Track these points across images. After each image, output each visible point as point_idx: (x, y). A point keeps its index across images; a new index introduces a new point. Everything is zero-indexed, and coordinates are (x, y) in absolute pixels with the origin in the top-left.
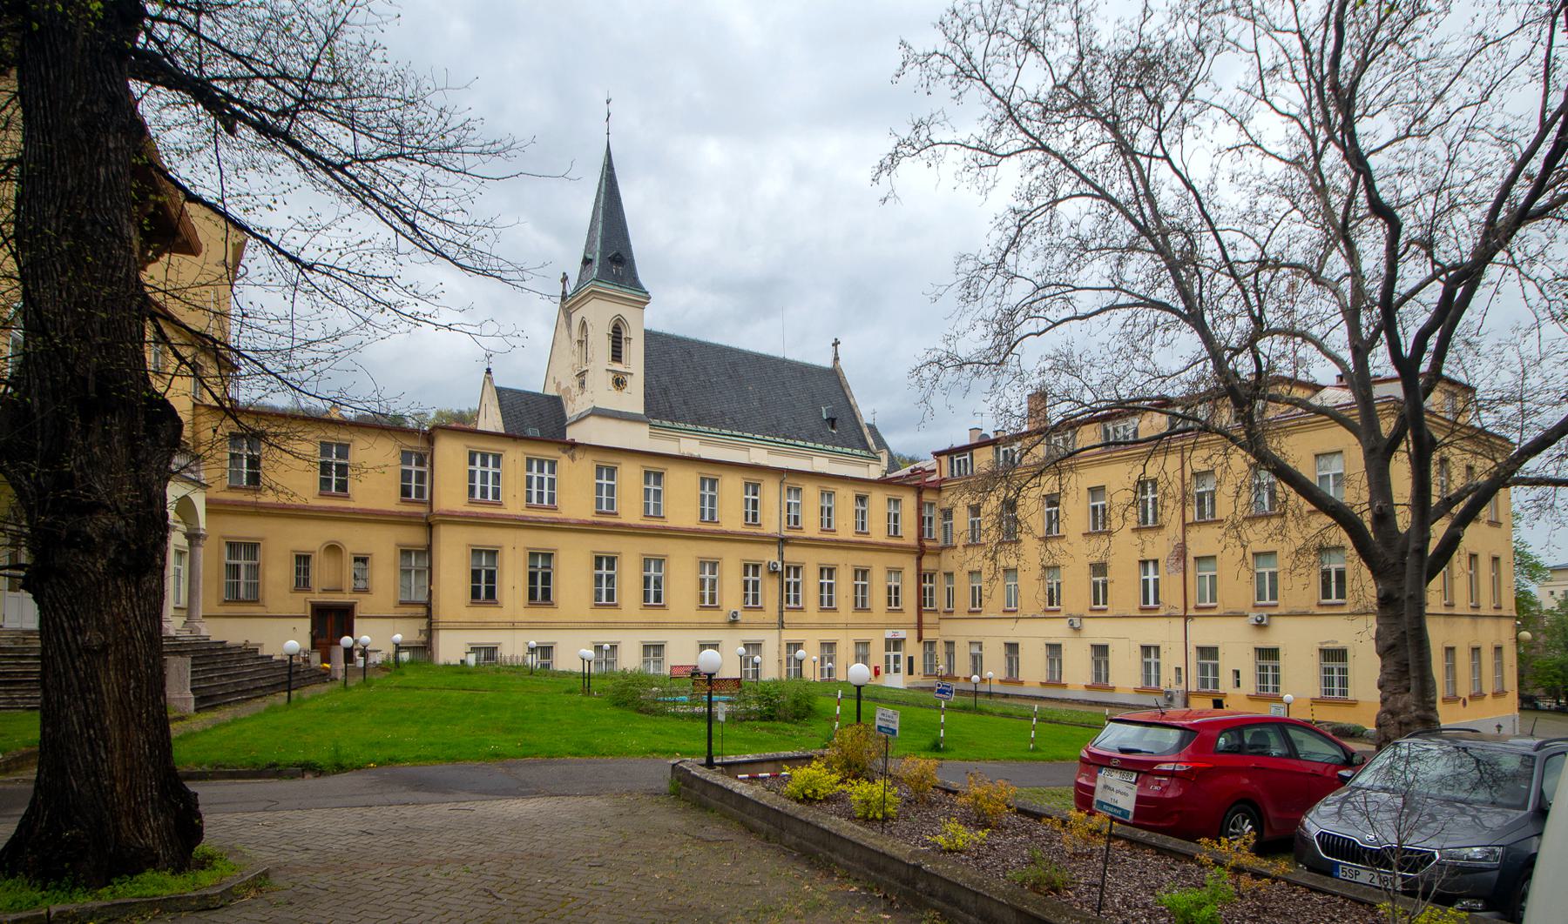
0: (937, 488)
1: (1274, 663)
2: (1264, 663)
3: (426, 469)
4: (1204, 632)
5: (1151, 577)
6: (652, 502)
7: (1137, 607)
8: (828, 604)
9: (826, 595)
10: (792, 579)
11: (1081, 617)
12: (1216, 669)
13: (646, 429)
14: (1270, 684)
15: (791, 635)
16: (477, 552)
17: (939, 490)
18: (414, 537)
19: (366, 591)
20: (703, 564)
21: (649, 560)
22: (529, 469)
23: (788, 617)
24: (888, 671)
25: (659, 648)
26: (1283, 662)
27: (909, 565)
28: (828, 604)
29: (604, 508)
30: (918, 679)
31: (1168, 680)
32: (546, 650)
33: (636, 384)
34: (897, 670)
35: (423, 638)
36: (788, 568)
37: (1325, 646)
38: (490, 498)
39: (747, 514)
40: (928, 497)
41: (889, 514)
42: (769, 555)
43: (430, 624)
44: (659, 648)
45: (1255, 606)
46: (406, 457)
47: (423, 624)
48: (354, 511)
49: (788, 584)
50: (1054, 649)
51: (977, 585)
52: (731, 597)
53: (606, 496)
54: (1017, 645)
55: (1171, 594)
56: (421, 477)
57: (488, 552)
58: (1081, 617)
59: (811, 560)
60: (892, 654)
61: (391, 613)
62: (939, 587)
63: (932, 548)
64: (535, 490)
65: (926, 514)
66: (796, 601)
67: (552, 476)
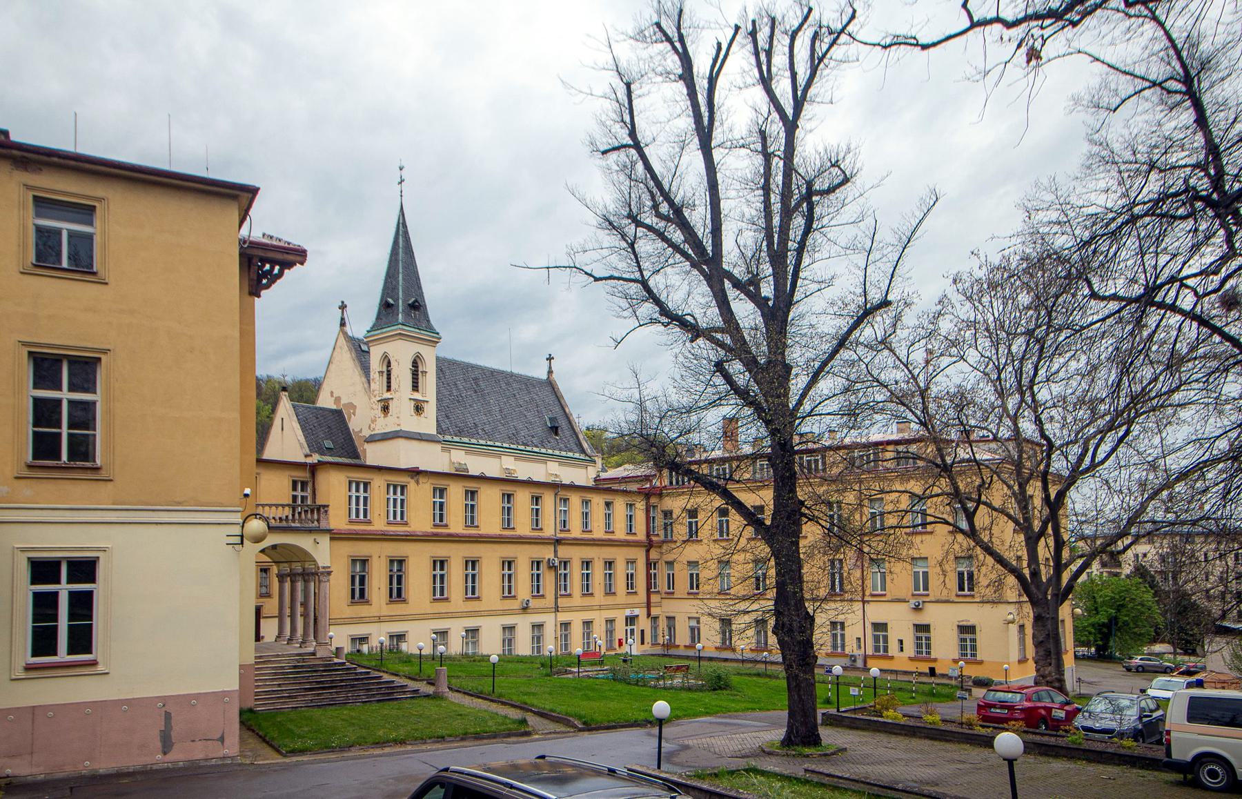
1: (927, 635)
2: (920, 634)
4: (877, 612)
10: (562, 571)
12: (886, 639)
14: (924, 650)
15: (563, 617)
17: (660, 495)
23: (562, 602)
26: (933, 634)
30: (647, 648)
31: (851, 647)
33: (431, 409)
37: (961, 624)
42: (547, 553)
45: (913, 595)
51: (695, 572)
59: (575, 555)
60: (629, 628)
62: (662, 573)
65: (652, 514)
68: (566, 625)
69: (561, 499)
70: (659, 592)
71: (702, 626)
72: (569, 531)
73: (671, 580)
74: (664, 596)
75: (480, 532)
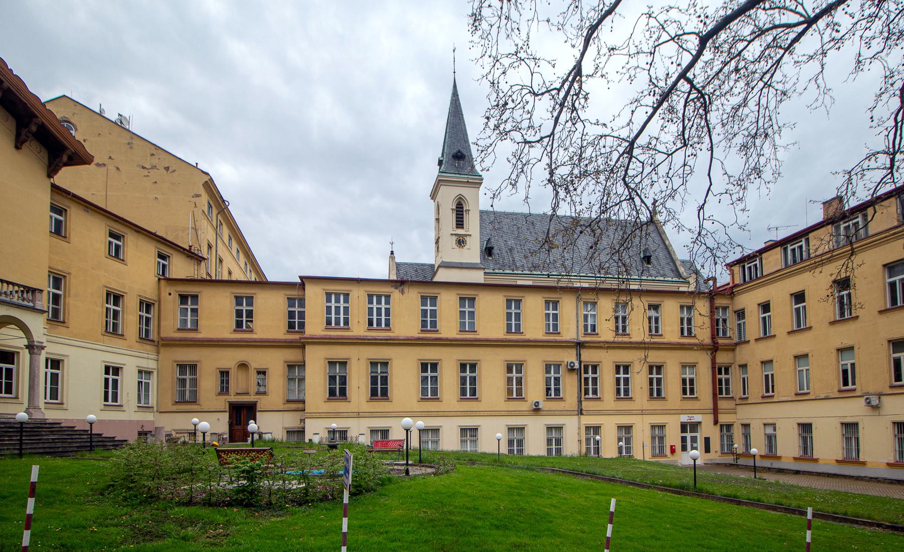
10: (590, 375)
18: (292, 355)
22: (371, 302)
24: (684, 448)
25: (474, 430)
27: (703, 362)
30: (715, 455)
36: (586, 367)
40: (720, 302)
42: (569, 357)
44: (474, 430)
49: (586, 379)
51: (770, 373)
52: (534, 389)
53: (429, 321)
57: (340, 363)
59: (607, 360)
60: (689, 435)
69: (586, 303)
70: (733, 398)
72: (597, 334)
75: (478, 337)
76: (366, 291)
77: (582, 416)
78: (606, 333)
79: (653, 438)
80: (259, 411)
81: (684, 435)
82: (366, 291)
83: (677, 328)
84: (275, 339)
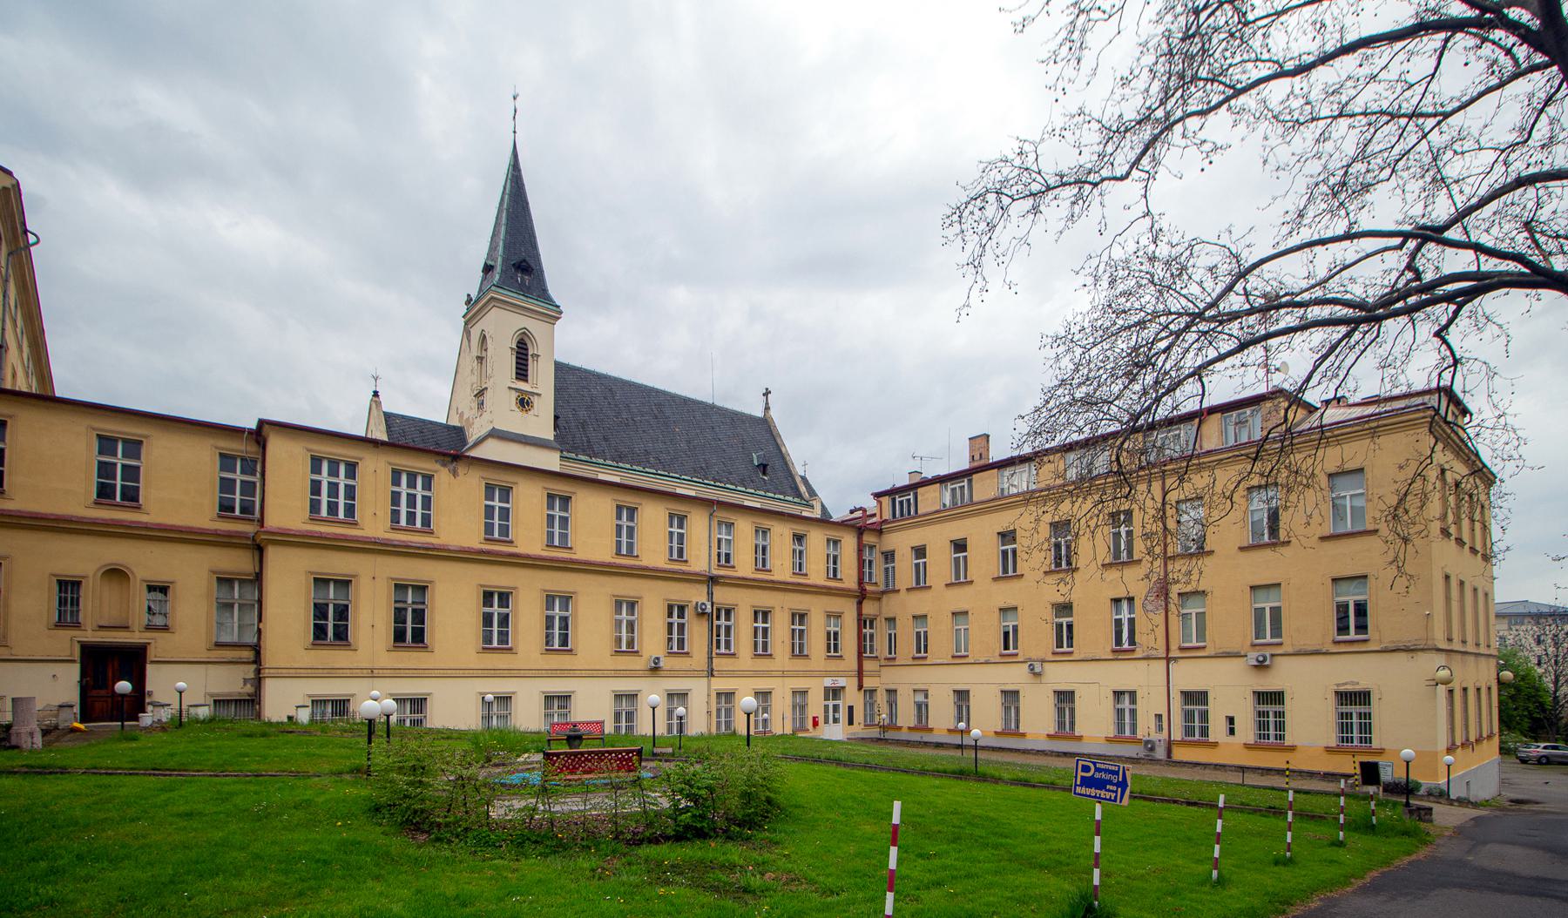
0: (879, 531)
1: (1278, 708)
3: (256, 479)
4: (1189, 675)
5: (1125, 615)
6: (557, 530)
7: (1108, 649)
8: (762, 650)
9: (760, 640)
10: (723, 622)
11: (1043, 661)
13: (557, 455)
14: (1272, 732)
15: (720, 684)
16: (321, 582)
17: (880, 532)
18: (239, 562)
19: (165, 628)
20: (618, 604)
21: (553, 597)
22: (396, 482)
24: (826, 722)
25: (565, 699)
27: (849, 609)
28: (762, 650)
29: (496, 535)
30: (858, 729)
32: (418, 703)
34: (836, 721)
35: (249, 689)
36: (719, 610)
37: (1342, 688)
38: (341, 515)
39: (671, 548)
40: (869, 539)
41: (828, 555)
42: (696, 595)
43: (258, 671)
44: (565, 699)
45: (1254, 645)
46: (227, 461)
47: (250, 671)
48: (146, 527)
49: (719, 627)
50: (1011, 697)
51: (922, 630)
52: (653, 640)
53: (498, 521)
54: (967, 692)
55: (1149, 635)
56: (248, 488)
57: (336, 581)
58: (1043, 661)
59: (744, 602)
60: (831, 703)
61: (204, 656)
62: (880, 633)
63: (873, 592)
64: (404, 509)
65: (866, 557)
66: (728, 646)
67: (427, 493)
68: (728, 696)
69: (720, 523)
71: (930, 701)
72: (734, 567)
73: (892, 640)
74: (883, 663)
76: (390, 464)
77: (713, 679)
78: (744, 565)
79: (794, 707)
80: (152, 662)
81: (827, 703)
82: (390, 464)
83: (823, 567)
84: (192, 528)
